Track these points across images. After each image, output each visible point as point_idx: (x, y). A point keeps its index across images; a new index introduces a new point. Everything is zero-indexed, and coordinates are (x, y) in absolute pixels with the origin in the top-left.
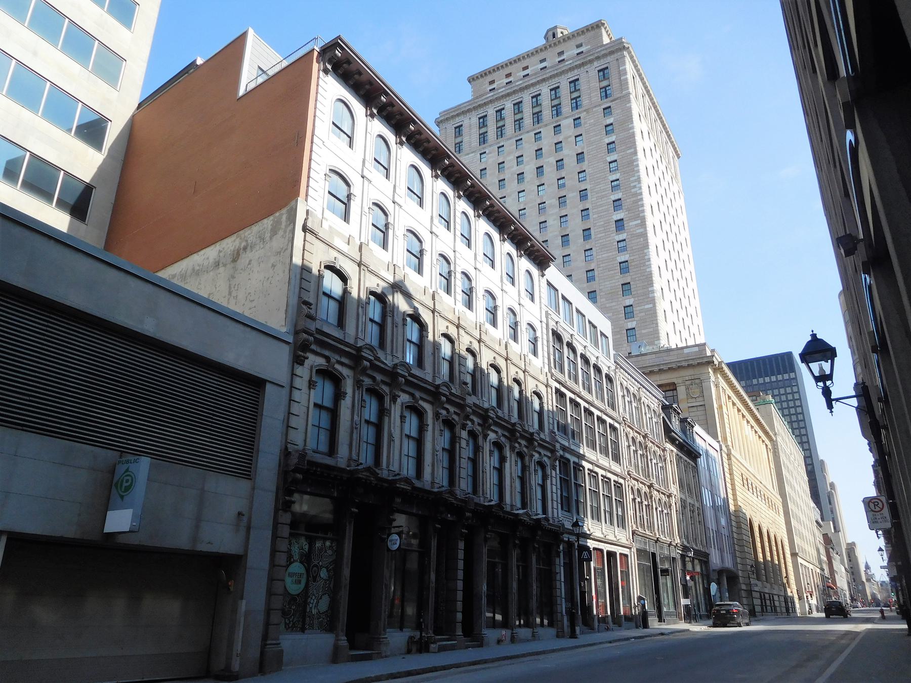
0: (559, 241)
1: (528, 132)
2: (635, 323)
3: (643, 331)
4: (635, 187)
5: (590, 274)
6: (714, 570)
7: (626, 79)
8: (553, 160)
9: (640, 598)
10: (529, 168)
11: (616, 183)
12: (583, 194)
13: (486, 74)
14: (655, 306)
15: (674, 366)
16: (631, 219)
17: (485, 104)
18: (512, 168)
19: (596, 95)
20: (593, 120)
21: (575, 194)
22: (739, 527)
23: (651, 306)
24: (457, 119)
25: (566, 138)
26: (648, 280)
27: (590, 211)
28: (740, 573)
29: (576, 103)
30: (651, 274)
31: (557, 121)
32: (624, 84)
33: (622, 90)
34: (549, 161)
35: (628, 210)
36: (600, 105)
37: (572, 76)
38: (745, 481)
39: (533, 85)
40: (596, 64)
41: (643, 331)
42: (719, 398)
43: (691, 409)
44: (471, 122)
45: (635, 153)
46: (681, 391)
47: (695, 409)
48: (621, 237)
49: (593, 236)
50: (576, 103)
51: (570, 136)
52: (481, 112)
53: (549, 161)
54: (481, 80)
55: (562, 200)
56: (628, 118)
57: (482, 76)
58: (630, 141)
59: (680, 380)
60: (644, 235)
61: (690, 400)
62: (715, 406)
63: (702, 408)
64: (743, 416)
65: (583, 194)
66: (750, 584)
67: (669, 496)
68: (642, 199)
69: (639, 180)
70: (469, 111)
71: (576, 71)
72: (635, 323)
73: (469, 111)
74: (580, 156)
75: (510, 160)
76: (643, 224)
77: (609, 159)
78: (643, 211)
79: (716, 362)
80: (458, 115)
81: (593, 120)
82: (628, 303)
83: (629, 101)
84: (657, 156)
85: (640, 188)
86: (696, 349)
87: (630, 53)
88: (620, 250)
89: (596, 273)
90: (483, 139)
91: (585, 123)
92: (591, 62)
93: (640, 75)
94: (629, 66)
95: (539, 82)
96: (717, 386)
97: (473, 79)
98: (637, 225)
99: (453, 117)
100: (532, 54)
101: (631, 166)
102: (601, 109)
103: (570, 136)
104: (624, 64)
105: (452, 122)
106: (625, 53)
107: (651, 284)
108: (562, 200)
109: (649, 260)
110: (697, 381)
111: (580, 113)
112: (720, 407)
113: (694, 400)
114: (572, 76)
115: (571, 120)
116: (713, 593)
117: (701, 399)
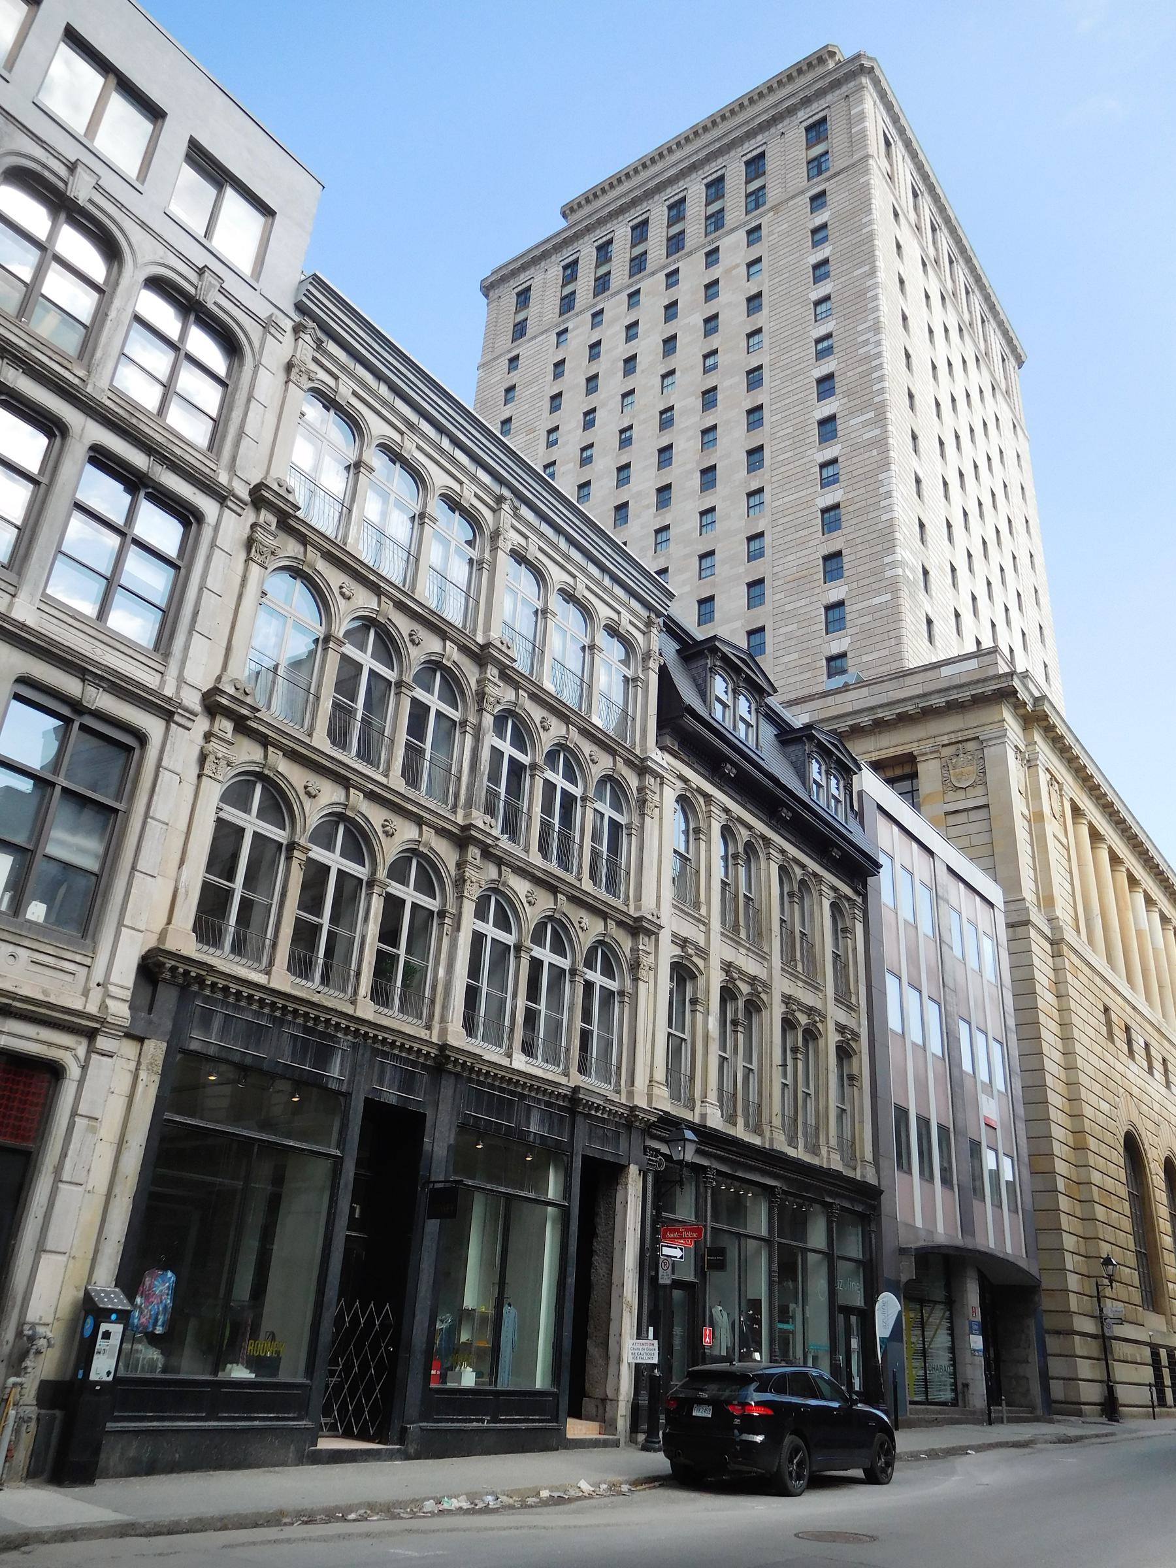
0: (697, 478)
2: (848, 640)
3: (865, 658)
4: (866, 343)
5: (755, 545)
6: (903, 1251)
7: (864, 130)
8: (697, 320)
9: (90, 1310)
10: (648, 346)
11: (825, 344)
12: (754, 377)
14: (896, 598)
15: (909, 708)
16: (852, 413)
18: (615, 348)
20: (787, 225)
21: (736, 379)
22: (1080, 1147)
23: (888, 597)
24: (523, 277)
25: (728, 271)
26: (884, 538)
27: (766, 412)
28: (1073, 1282)
30: (891, 525)
32: (857, 140)
34: (690, 322)
35: (849, 393)
36: (803, 192)
37: (750, 148)
38: (1119, 1032)
39: (671, 181)
40: (801, 114)
41: (865, 658)
42: (1032, 794)
43: (952, 820)
44: (546, 283)
45: (873, 272)
46: (929, 772)
47: (962, 818)
48: (828, 455)
49: (767, 463)
51: (737, 266)
52: (567, 255)
53: (690, 322)
55: (709, 397)
56: (865, 205)
58: (863, 252)
59: (926, 746)
60: (881, 443)
61: (951, 796)
62: (1019, 806)
63: (981, 814)
64: (1133, 881)
65: (754, 377)
66: (1101, 1319)
67: (638, 928)
68: (880, 366)
69: (877, 328)
71: (759, 137)
72: (848, 640)
73: (545, 255)
74: (754, 302)
75: (612, 335)
76: (880, 420)
78: (882, 391)
79: (1023, 695)
80: (524, 268)
81: (787, 225)
82: (834, 596)
83: (867, 172)
85: (878, 343)
86: (973, 664)
87: (877, 83)
88: (825, 483)
89: (767, 539)
90: (567, 303)
91: (770, 233)
92: (791, 111)
93: (902, 131)
94: (870, 105)
96: (1030, 763)
97: (572, 210)
98: (865, 424)
99: (514, 273)
101: (863, 300)
102: (805, 199)
103: (737, 266)
104: (861, 101)
105: (513, 283)
106: (865, 81)
107: (891, 548)
108: (709, 397)
109: (889, 495)
110: (971, 746)
111: (761, 215)
112: (1036, 819)
113: (960, 794)
114: (750, 148)
115: (741, 235)
116: (883, 1328)
117: (980, 790)
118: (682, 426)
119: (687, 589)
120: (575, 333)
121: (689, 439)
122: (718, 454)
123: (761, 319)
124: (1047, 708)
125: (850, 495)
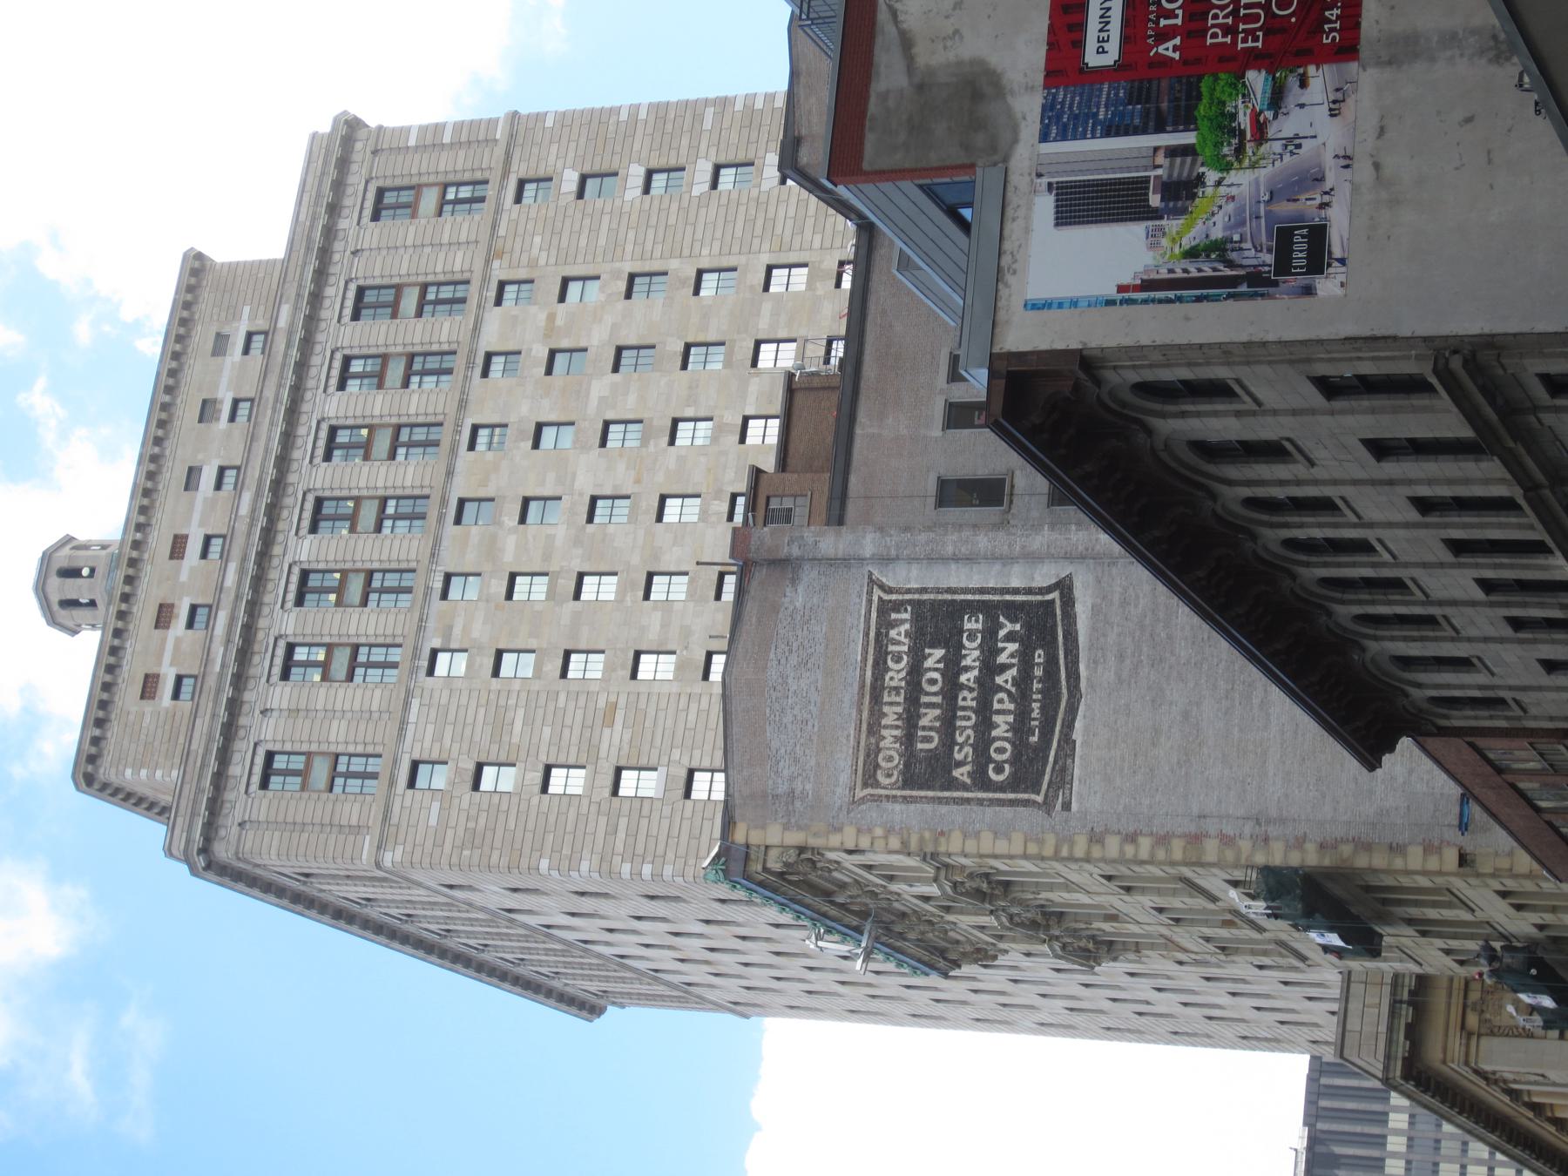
1: (450, 473)
13: (103, 705)
17: (249, 630)
19: (463, 225)
29: (436, 296)
31: (470, 365)
33: (491, 141)
50: (436, 296)
51: (551, 318)
54: (114, 731)
57: (100, 723)
70: (234, 706)
73: (234, 706)
77: (701, 186)
100: (143, 510)
103: (551, 318)
120: (457, 631)
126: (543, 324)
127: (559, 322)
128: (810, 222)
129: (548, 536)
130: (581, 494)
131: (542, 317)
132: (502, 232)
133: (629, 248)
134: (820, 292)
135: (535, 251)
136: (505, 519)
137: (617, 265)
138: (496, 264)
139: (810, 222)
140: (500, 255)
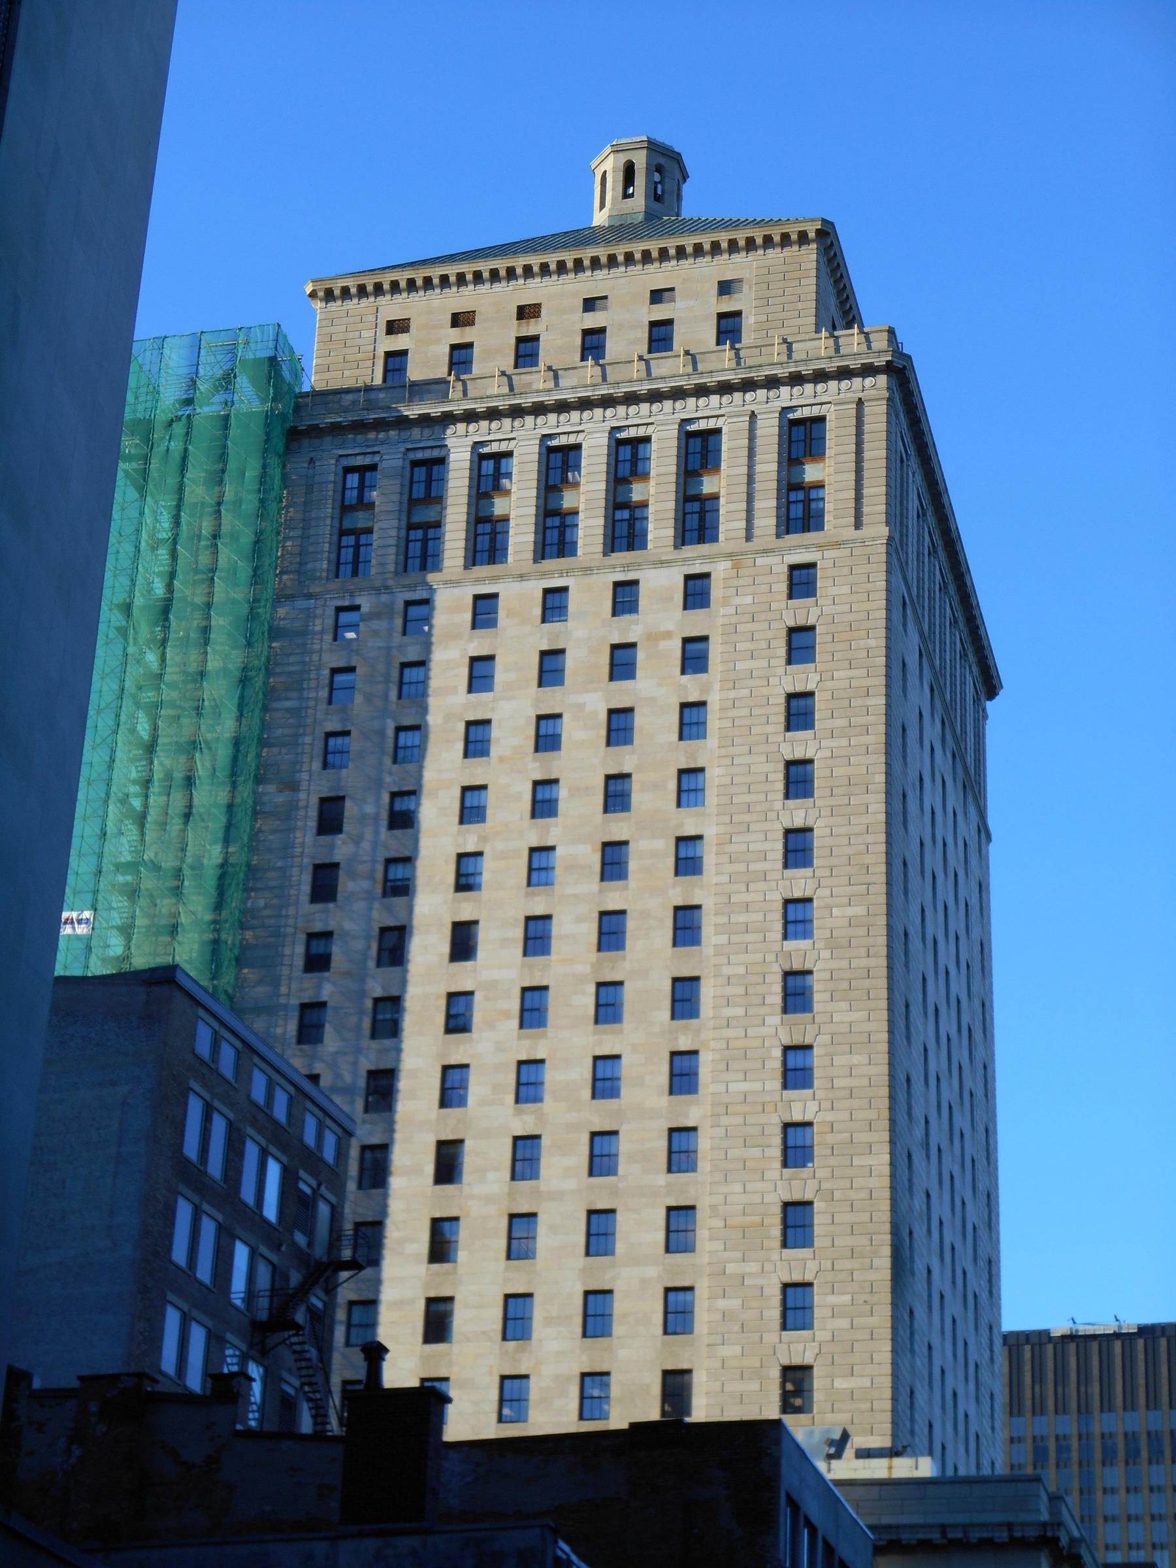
51: (668, 635)
84: (932, 732)
95: (585, 404)
103: (668, 635)
118: (569, 890)
119: (571, 1184)
121: (579, 920)
122: (627, 965)
123: (705, 752)
124: (1083, 1551)
125: (829, 1117)
126: (662, 629)
127: (663, 645)
128: (742, 867)
129: (456, 688)
130: (493, 709)
131: (670, 626)
132: (760, 561)
133: (732, 694)
134: (671, 892)
135: (738, 601)
136: (475, 643)
137: (717, 686)
138: (729, 564)
139: (742, 867)
140: (736, 567)
